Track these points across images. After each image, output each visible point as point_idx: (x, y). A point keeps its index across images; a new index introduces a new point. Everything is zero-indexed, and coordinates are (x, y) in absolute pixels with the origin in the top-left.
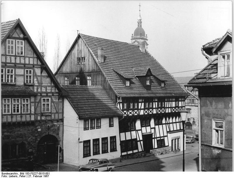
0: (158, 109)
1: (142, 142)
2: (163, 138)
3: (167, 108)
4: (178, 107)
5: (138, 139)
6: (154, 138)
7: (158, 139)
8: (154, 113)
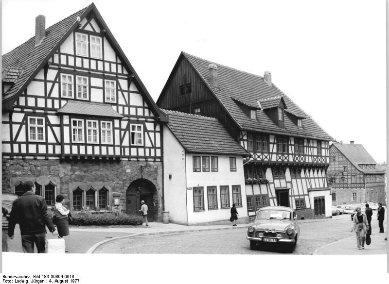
0: (295, 156)
1: (275, 200)
2: (303, 197)
3: (306, 155)
4: (321, 157)
5: (270, 196)
6: (292, 196)
7: (296, 197)
8: (290, 161)
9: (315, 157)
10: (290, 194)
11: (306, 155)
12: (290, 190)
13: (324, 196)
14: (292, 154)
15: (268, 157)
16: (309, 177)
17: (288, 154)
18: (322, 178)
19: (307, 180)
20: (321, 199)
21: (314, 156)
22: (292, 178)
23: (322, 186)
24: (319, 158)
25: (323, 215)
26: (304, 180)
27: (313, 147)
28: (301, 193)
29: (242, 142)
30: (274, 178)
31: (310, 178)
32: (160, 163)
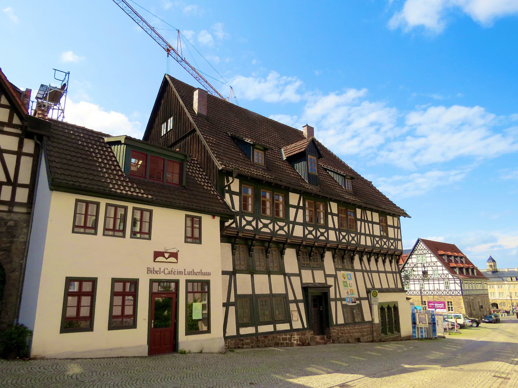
0: (340, 233)
1: (302, 306)
3: (361, 234)
4: (389, 239)
5: (291, 297)
6: (336, 300)
9: (377, 239)
10: (332, 295)
11: (361, 234)
12: (332, 290)
14: (334, 229)
15: (286, 228)
16: (368, 269)
17: (327, 229)
19: (365, 274)
21: (374, 236)
22: (336, 269)
24: (385, 240)
27: (373, 223)
29: (227, 196)
30: (301, 267)
31: (371, 272)
32: (25, 217)
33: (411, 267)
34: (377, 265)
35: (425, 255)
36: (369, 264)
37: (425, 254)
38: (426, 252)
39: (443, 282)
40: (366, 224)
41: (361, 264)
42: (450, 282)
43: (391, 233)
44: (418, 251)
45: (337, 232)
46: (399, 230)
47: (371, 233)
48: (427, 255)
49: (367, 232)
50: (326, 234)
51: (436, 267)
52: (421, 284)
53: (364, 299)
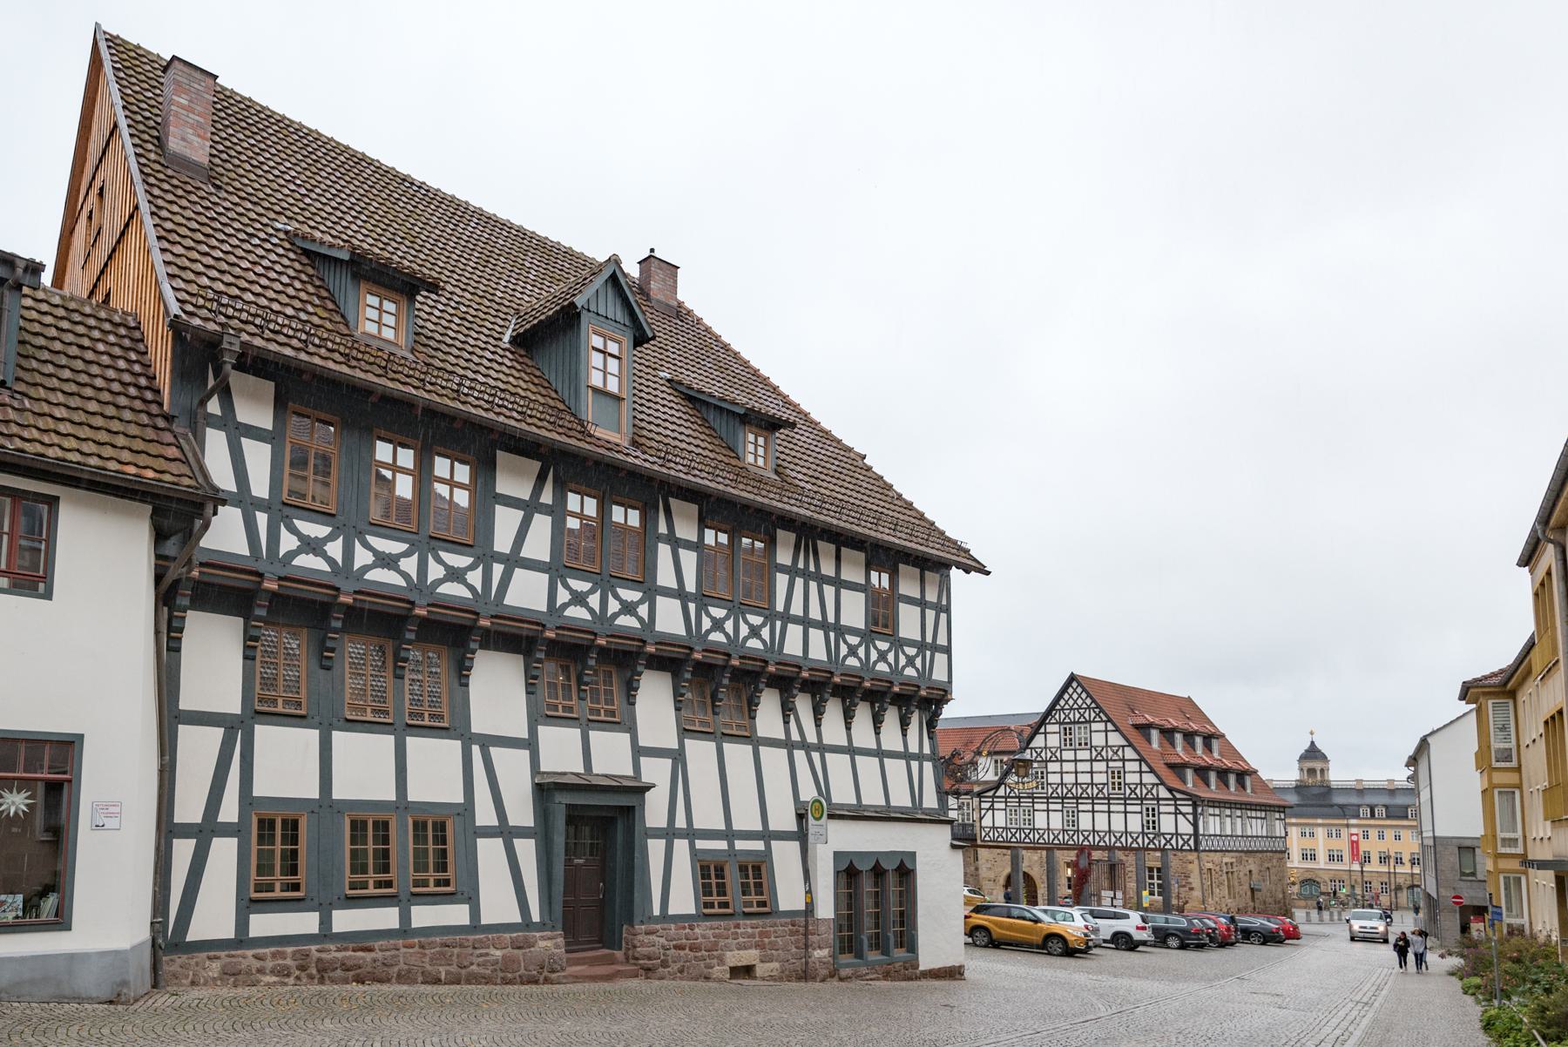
1: (527, 850)
2: (759, 845)
3: (787, 618)
4: (898, 644)
5: (485, 815)
6: (670, 834)
7: (701, 844)
8: (659, 627)
9: (853, 640)
11: (787, 618)
13: (913, 854)
14: (680, 594)
16: (812, 738)
18: (906, 756)
19: (799, 755)
20: (889, 866)
21: (841, 631)
22: (684, 732)
23: (901, 798)
25: (899, 953)
26: (774, 759)
28: (746, 818)
31: (823, 748)
33: (1042, 761)
34: (848, 728)
35: (1088, 725)
36: (818, 724)
37: (1089, 722)
38: (1093, 715)
39: (1138, 808)
40: (813, 585)
41: (786, 722)
42: (1163, 809)
43: (909, 622)
44: (1067, 712)
45: (692, 607)
46: (943, 616)
47: (831, 619)
48: (1095, 726)
49: (815, 613)
50: (643, 610)
51: (1120, 764)
52: (1068, 812)
53: (783, 836)
